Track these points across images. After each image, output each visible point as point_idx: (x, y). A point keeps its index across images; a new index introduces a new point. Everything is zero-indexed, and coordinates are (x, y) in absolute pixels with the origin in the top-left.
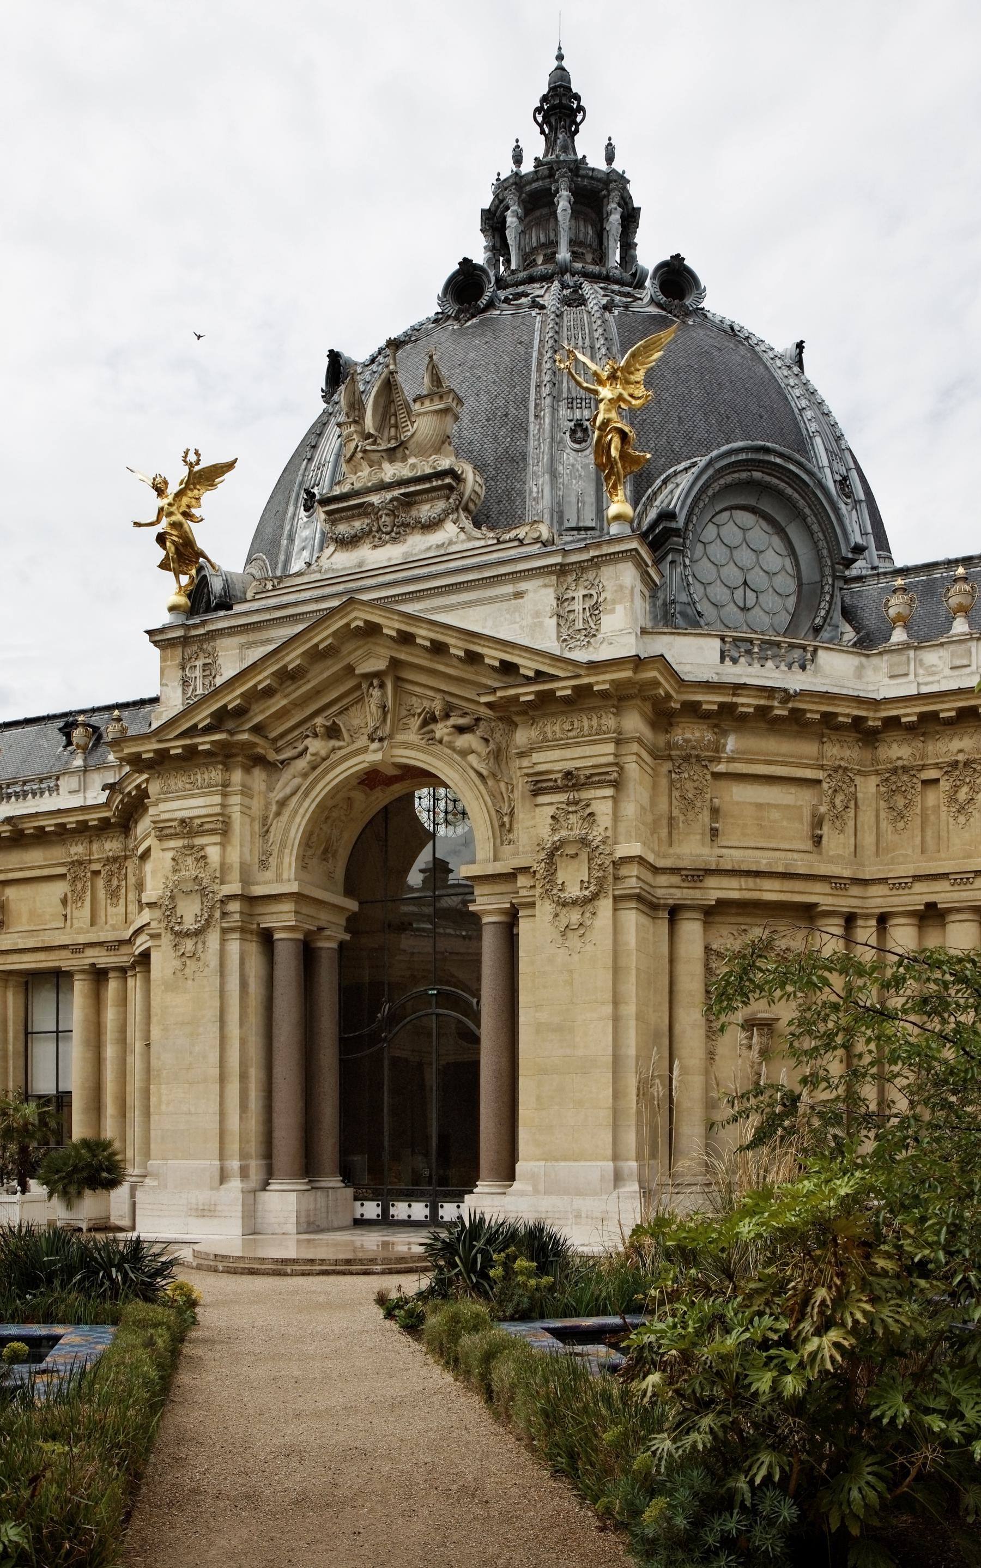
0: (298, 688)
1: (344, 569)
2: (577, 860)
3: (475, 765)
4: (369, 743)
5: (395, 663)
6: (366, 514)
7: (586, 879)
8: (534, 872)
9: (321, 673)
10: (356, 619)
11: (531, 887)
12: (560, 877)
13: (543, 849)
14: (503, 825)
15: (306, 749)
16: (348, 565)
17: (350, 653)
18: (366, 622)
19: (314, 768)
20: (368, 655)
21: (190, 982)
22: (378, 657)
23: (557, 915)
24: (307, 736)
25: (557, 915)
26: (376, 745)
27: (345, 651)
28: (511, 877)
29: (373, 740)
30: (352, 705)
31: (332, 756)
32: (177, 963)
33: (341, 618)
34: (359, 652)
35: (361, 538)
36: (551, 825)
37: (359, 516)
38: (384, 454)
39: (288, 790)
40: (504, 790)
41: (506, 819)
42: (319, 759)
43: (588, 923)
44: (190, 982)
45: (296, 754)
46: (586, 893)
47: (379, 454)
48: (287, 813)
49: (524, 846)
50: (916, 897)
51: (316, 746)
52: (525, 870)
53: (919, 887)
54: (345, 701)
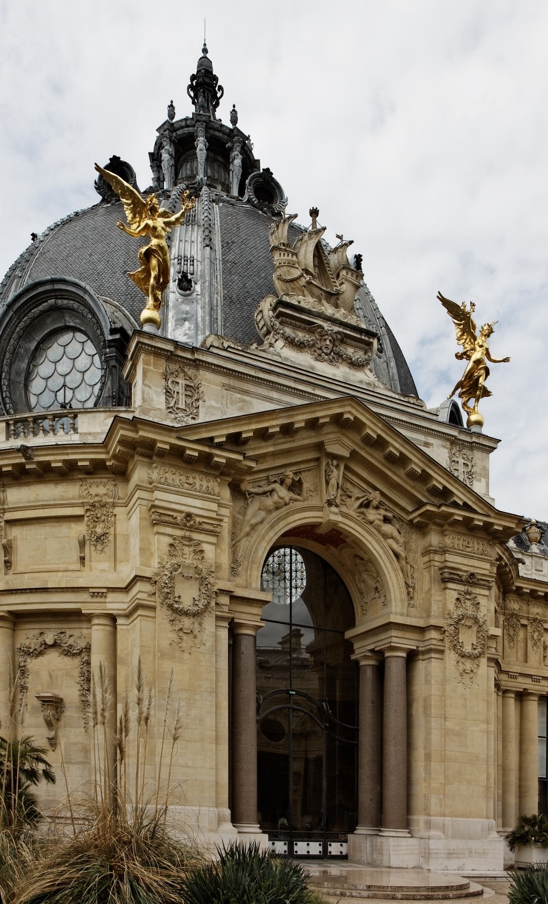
0: (285, 443)
1: (299, 364)
2: (469, 631)
3: (395, 546)
4: (326, 505)
5: (354, 453)
6: (311, 332)
7: (475, 643)
8: (445, 631)
9: (304, 439)
10: (349, 412)
11: (440, 640)
12: (462, 638)
13: (451, 618)
14: (408, 593)
15: (272, 491)
16: (303, 363)
17: (328, 434)
18: (356, 418)
19: (277, 508)
20: (338, 441)
21: (186, 655)
22: (344, 446)
23: (458, 662)
24: (275, 482)
25: (458, 662)
26: (334, 509)
27: (326, 430)
28: (422, 630)
29: (330, 503)
30: (304, 471)
31: (291, 504)
32: (174, 636)
33: (340, 407)
34: (331, 436)
35: (305, 346)
36: (455, 603)
37: (304, 330)
38: (323, 294)
39: (259, 519)
40: (409, 569)
41: (411, 590)
42: (283, 503)
43: (475, 671)
44: (186, 655)
45: (261, 492)
46: (476, 652)
47: (320, 292)
48: (255, 536)
49: (435, 612)
50: (518, 684)
51: (283, 492)
52: (437, 628)
53: (520, 679)
54: (302, 466)
